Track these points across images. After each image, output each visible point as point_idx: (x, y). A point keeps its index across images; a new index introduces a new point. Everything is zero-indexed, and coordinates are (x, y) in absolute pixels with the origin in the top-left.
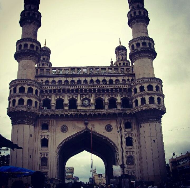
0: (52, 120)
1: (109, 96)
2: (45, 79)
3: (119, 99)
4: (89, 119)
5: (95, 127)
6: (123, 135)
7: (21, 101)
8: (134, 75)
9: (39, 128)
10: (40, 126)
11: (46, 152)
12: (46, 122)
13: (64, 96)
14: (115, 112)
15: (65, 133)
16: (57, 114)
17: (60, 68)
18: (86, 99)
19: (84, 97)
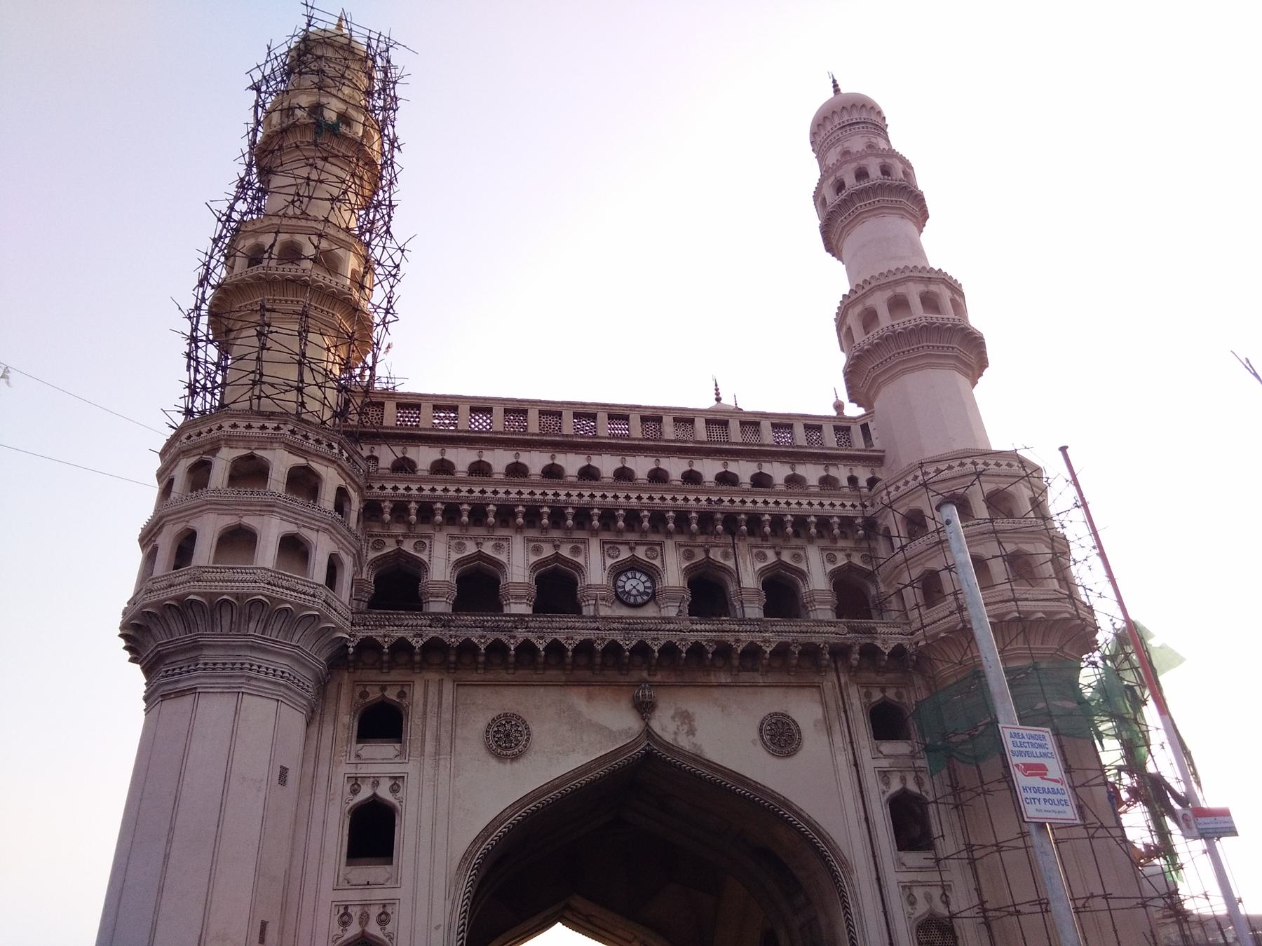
0: (433, 676)
1: (763, 557)
2: (386, 455)
3: (817, 572)
4: (658, 678)
5: (696, 724)
6: (871, 781)
7: (238, 540)
8: (877, 460)
9: (342, 734)
10: (347, 720)
11: (378, 894)
12: (392, 695)
14: (813, 640)
15: (516, 765)
16: (468, 640)
17: (480, 405)
18: (634, 566)
19: (625, 554)
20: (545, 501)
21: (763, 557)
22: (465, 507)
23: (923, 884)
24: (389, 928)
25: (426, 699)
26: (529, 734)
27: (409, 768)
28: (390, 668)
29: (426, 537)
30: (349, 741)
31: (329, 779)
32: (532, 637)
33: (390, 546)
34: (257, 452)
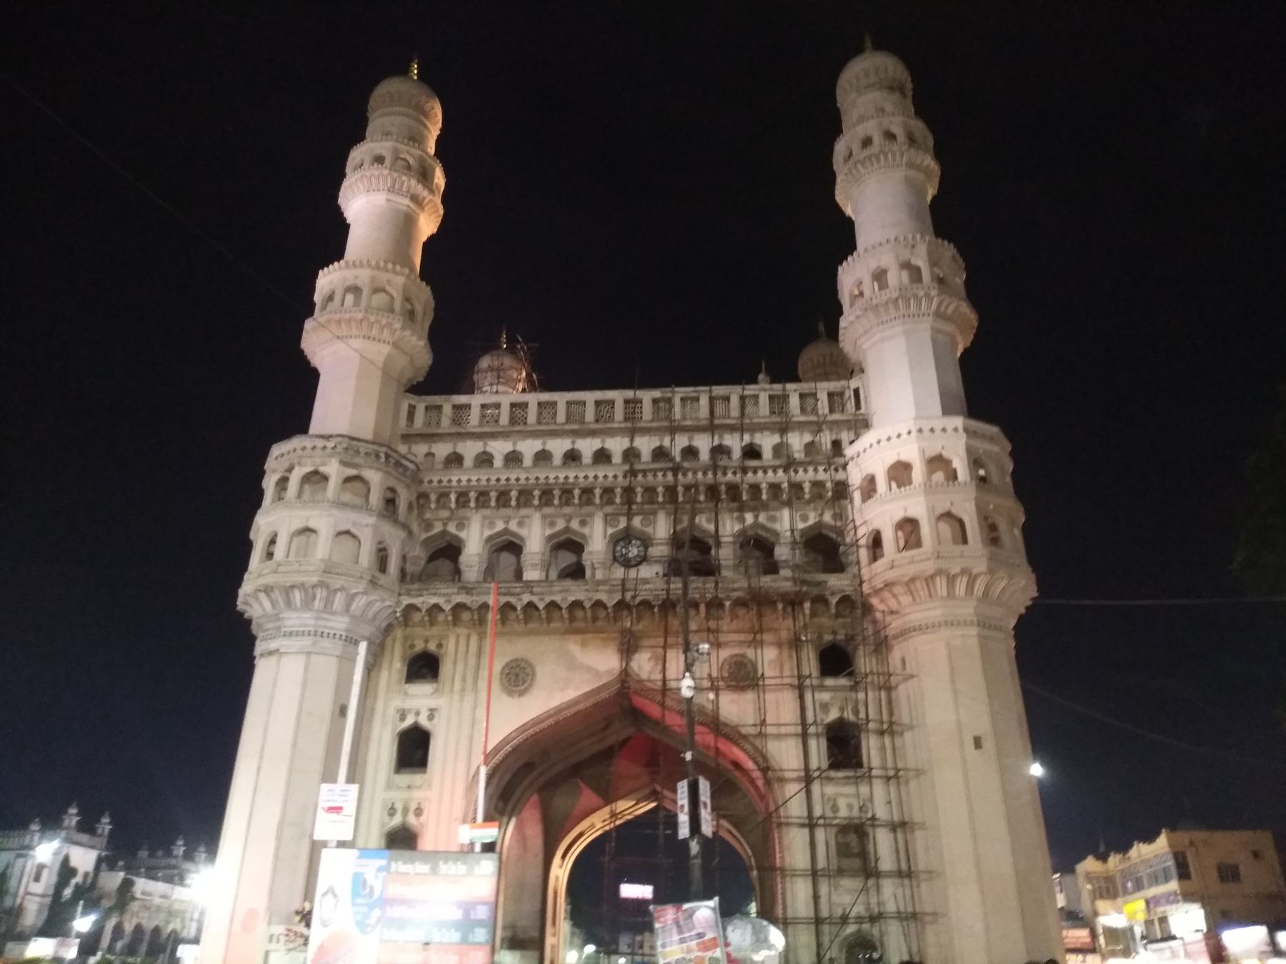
0: (462, 631)
2: (442, 450)
9: (395, 677)
12: (432, 647)
15: (523, 699)
19: (623, 524)
21: (742, 520)
23: (847, 796)
24: (423, 818)
25: (456, 649)
26: (534, 674)
27: (440, 702)
30: (399, 682)
32: (535, 599)
33: (438, 528)
34: (322, 469)
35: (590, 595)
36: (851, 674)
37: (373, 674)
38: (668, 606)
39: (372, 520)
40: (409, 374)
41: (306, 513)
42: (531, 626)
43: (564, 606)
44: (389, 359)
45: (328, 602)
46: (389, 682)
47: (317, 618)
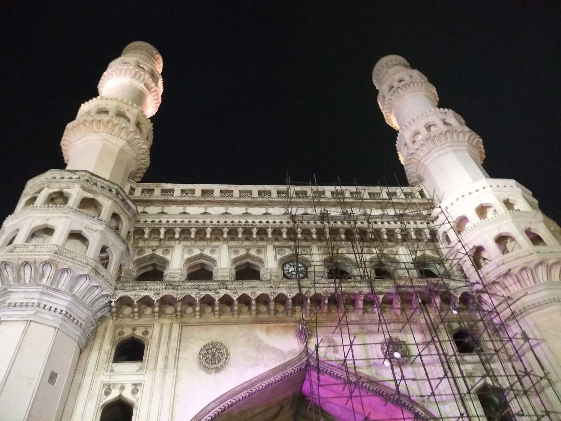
0: (166, 321)
9: (104, 357)
13: (217, 249)
15: (218, 375)
16: (189, 296)
19: (288, 252)
20: (240, 225)
22: (193, 229)
26: (227, 354)
27: (145, 378)
28: (140, 317)
29: (170, 247)
30: (107, 361)
31: (91, 387)
32: (230, 293)
33: (148, 252)
34: (65, 190)
35: (273, 290)
36: (480, 352)
37: (84, 355)
38: (334, 300)
39: (101, 227)
40: (133, 168)
41: (49, 215)
42: (223, 317)
43: (254, 298)
44: (122, 150)
45: (55, 280)
46: (97, 363)
47: (42, 293)
